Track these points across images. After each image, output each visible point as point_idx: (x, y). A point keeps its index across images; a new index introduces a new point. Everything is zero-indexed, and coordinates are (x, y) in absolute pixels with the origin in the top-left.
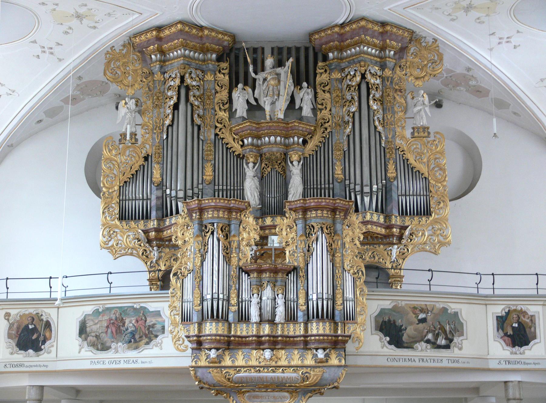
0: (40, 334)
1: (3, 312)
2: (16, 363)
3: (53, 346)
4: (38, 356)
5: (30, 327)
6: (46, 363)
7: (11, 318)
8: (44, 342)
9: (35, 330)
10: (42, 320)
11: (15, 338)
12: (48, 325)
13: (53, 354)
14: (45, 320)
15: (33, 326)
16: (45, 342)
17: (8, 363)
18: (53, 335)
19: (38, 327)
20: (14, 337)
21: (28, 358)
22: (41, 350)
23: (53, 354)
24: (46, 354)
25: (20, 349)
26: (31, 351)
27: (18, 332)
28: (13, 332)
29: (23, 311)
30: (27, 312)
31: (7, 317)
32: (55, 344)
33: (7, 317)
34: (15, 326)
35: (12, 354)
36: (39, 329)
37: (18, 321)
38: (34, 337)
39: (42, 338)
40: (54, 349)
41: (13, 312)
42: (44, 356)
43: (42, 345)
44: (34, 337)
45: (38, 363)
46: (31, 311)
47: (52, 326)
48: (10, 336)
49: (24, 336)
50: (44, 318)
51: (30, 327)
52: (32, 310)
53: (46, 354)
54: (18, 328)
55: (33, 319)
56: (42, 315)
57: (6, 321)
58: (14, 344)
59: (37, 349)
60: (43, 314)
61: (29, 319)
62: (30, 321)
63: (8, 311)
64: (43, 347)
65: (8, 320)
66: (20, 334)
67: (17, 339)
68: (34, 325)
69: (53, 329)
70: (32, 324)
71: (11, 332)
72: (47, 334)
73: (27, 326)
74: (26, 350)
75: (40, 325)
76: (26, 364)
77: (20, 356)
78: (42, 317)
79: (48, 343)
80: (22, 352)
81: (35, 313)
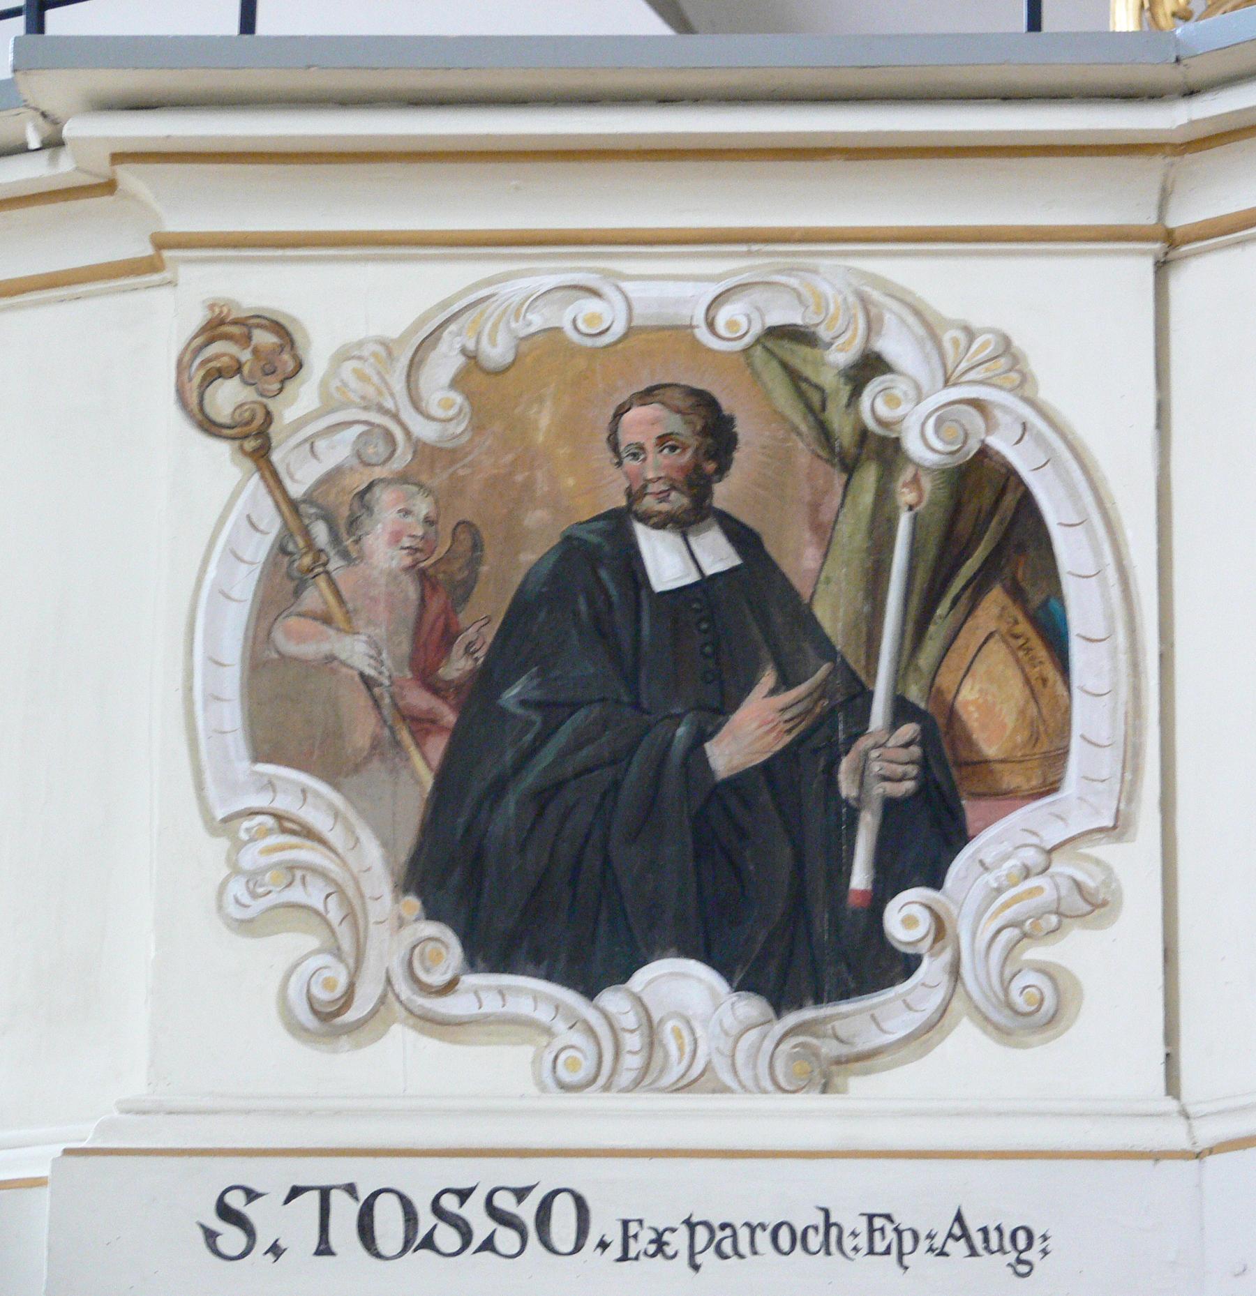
0: (861, 696)
1: (167, 316)
2: (422, 1183)
3: (1094, 905)
4: (826, 1077)
5: (666, 562)
6: (994, 1198)
7: (297, 405)
8: (928, 834)
9: (748, 617)
10: (883, 450)
11: (385, 749)
12: (989, 537)
13: (1105, 1054)
14: (925, 447)
15: (716, 554)
16: (954, 836)
17: (273, 1178)
18: (1092, 716)
19: (798, 558)
20: (363, 727)
21: (665, 1078)
22: (878, 966)
23: (1105, 1054)
24: (965, 1040)
25: (491, 949)
26: (680, 986)
27: (431, 641)
28: (355, 651)
29: (528, 298)
30: (604, 316)
31: (227, 398)
32: (1133, 864)
33: (227, 398)
34: (383, 552)
35: (329, 1019)
36: (833, 614)
37: (426, 454)
38: (747, 736)
39: (878, 765)
40: (1109, 964)
41: (347, 311)
42: (924, 1088)
43: (889, 881)
44: (747, 736)
45: (851, 1193)
46: (670, 289)
47: (1069, 550)
48: (286, 715)
49: (553, 710)
50: (919, 418)
51: (666, 562)
52: (674, 272)
53: (965, 1040)
54: (440, 582)
55: (716, 434)
56: (871, 366)
57: (220, 462)
58: (369, 857)
59: (801, 933)
60: (892, 346)
61: (643, 423)
62: (656, 465)
63: (256, 287)
64: (904, 919)
65: (255, 439)
66: (487, 681)
67: (423, 768)
68: (742, 536)
69: (1084, 607)
70: (682, 524)
71: (301, 641)
72: (988, 700)
73: (601, 553)
74: (591, 958)
75: (852, 532)
76: (615, 1195)
77: (493, 1067)
78: (875, 404)
79: (997, 849)
80: (530, 994)
81: (741, 320)
